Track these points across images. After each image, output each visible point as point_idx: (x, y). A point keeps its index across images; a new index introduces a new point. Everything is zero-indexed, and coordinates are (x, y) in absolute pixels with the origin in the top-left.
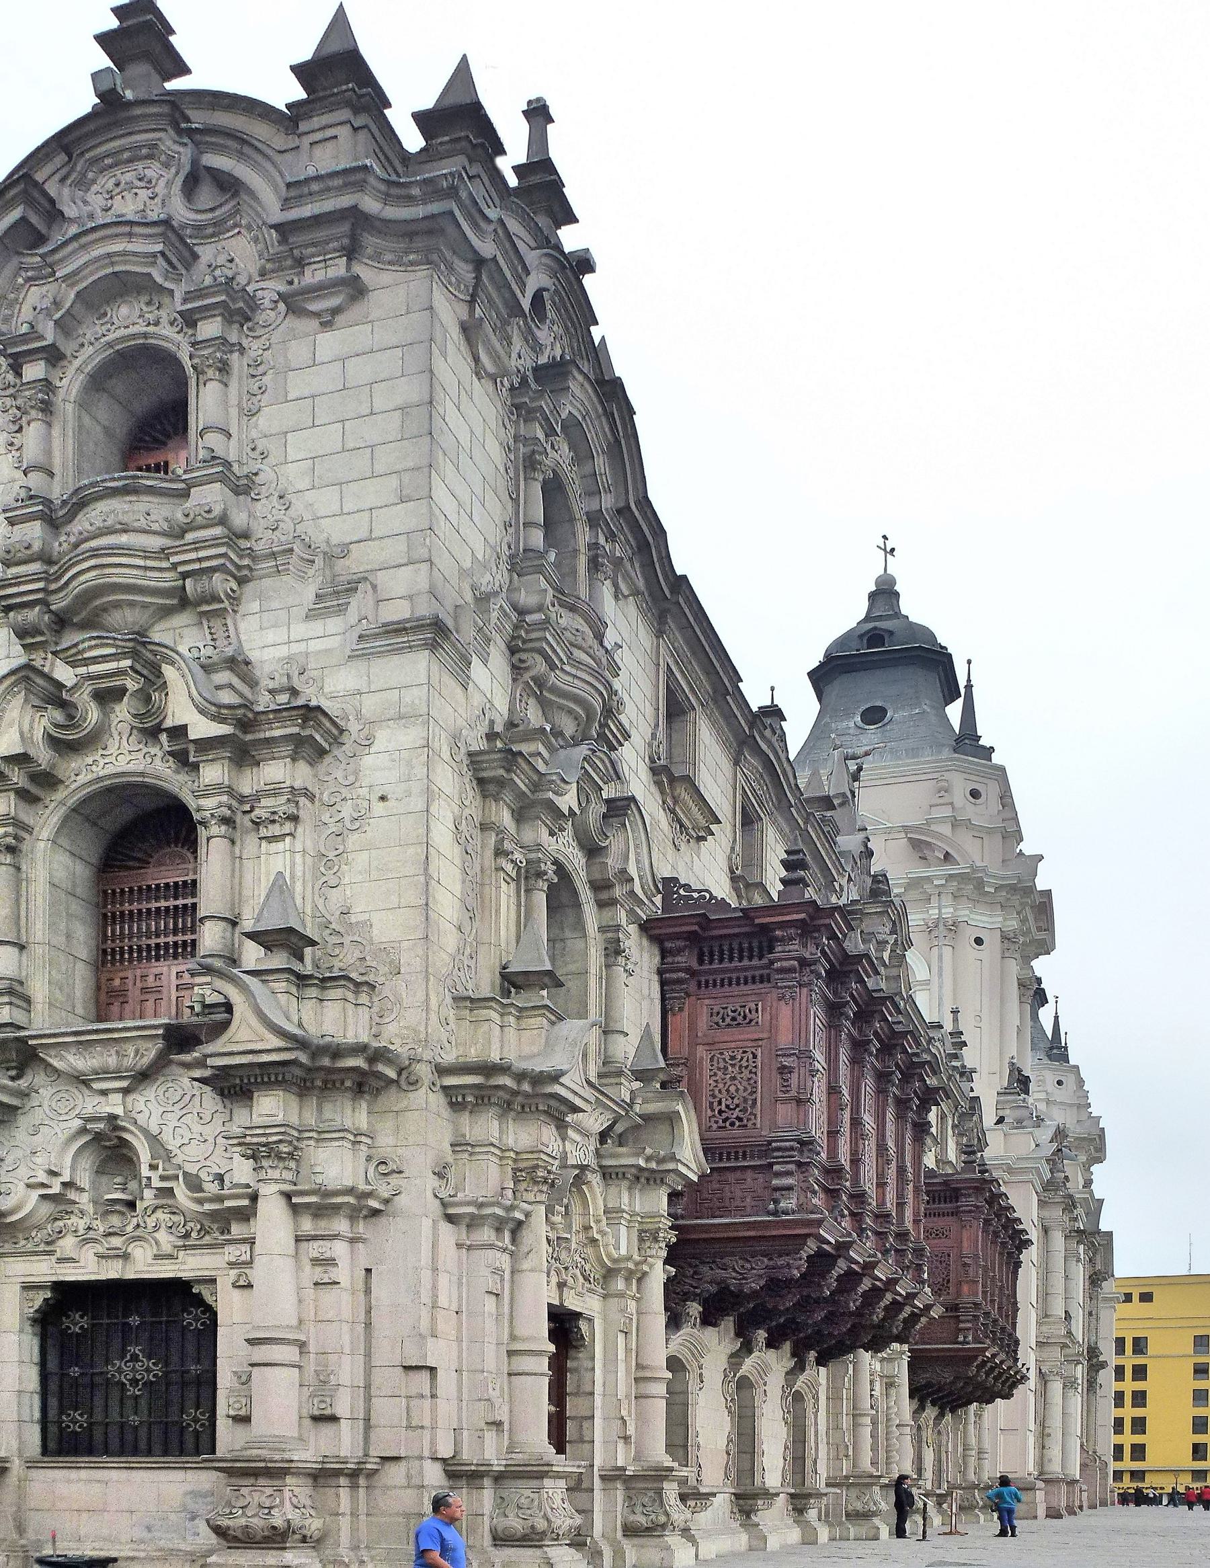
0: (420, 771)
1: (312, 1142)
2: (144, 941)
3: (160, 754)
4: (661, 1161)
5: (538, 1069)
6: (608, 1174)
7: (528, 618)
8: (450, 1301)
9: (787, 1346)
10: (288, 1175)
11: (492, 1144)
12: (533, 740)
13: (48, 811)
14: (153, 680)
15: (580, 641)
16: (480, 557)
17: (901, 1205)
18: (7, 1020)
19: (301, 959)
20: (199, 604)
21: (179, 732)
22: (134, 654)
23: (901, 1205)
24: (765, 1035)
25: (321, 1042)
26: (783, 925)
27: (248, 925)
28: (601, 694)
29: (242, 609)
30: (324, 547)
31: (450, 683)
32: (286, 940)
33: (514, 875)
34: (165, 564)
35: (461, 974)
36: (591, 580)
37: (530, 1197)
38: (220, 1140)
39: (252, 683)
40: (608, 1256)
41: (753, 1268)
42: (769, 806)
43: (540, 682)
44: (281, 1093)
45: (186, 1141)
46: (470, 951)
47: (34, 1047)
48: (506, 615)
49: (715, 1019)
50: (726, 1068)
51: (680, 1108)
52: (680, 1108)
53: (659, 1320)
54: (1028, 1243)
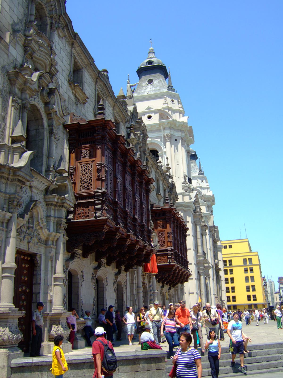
41: (91, 237)
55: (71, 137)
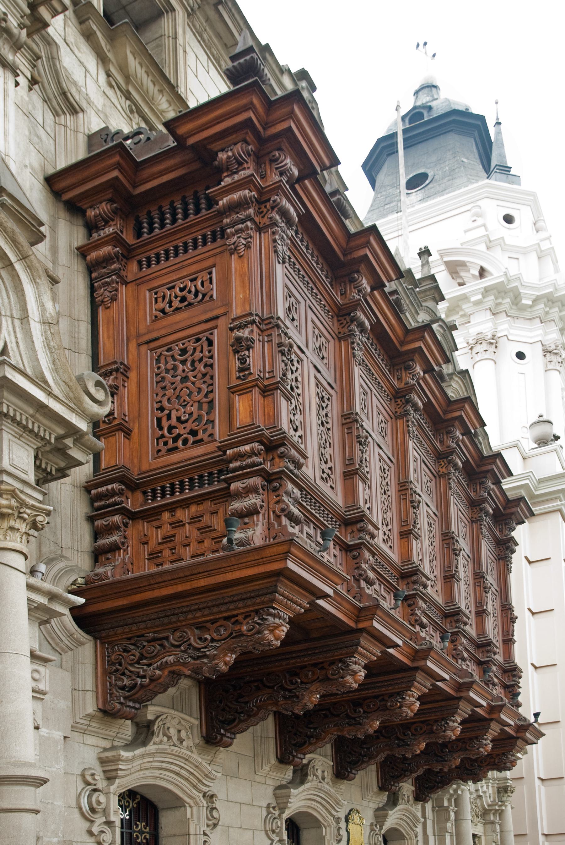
50: (175, 368)
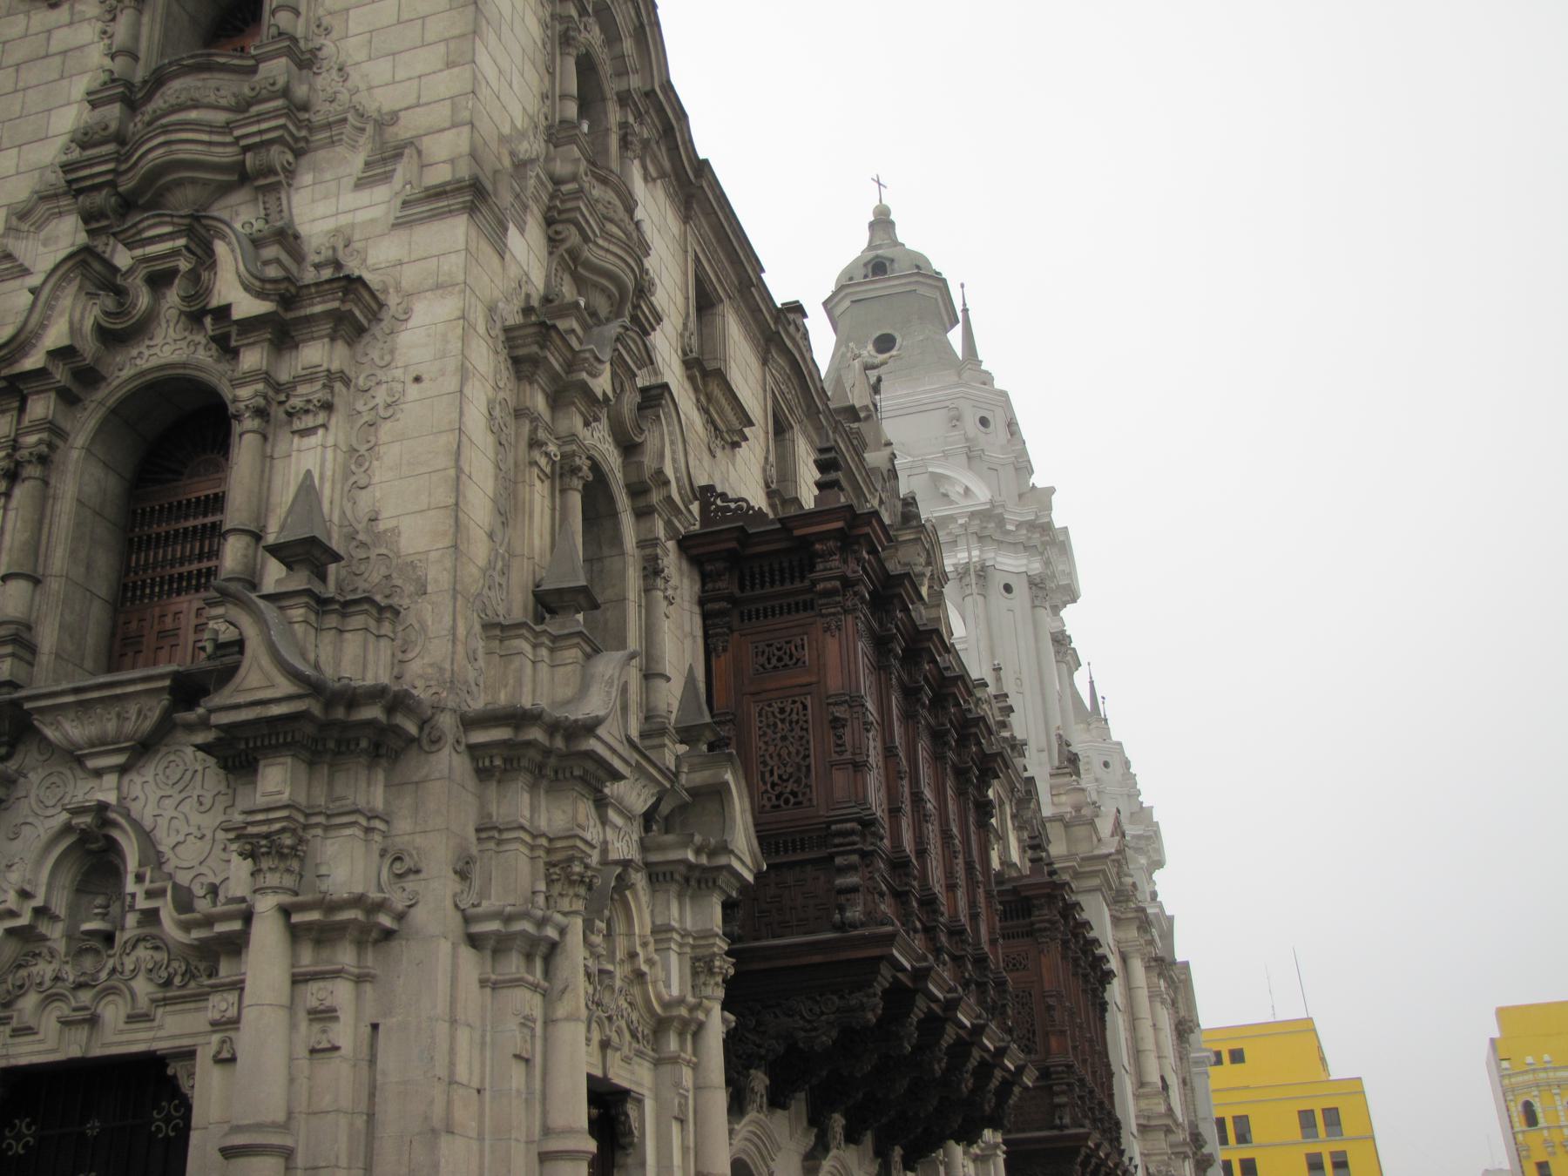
0: (455, 346)
1: (319, 831)
2: (168, 571)
3: (204, 341)
4: (712, 854)
5: (572, 718)
6: (658, 876)
7: (565, 188)
8: (471, 1074)
9: (868, 1139)
10: (289, 881)
11: (522, 828)
12: (567, 316)
13: (86, 414)
14: (205, 258)
15: (612, 214)
16: (519, 125)
17: (974, 917)
18: (5, 676)
19: (323, 577)
20: (256, 179)
21: (223, 312)
22: (190, 232)
23: (974, 917)
24: (814, 679)
25: (337, 685)
26: (823, 537)
27: (271, 539)
28: (633, 270)
29: (296, 183)
30: (375, 115)
31: (486, 249)
32: (308, 553)
33: (548, 470)
34: (228, 139)
35: (491, 594)
36: (622, 157)
37: (565, 904)
38: (221, 835)
39: (298, 256)
40: (659, 997)
41: (822, 1013)
42: (799, 412)
43: (574, 254)
44: (289, 760)
45: (181, 838)
46: (502, 562)
47: (29, 713)
48: (542, 183)
49: (762, 660)
50: (775, 725)
51: (729, 777)
52: (729, 777)
53: (719, 1099)
54: (1109, 975)
55: (709, 586)
